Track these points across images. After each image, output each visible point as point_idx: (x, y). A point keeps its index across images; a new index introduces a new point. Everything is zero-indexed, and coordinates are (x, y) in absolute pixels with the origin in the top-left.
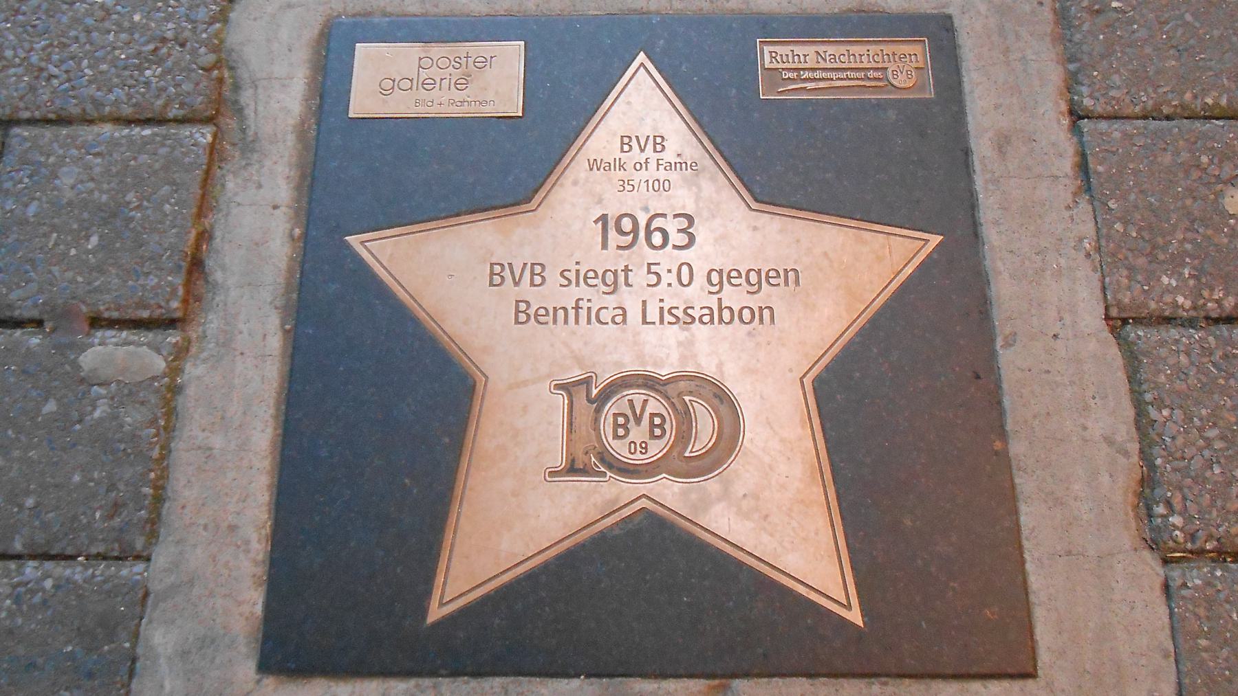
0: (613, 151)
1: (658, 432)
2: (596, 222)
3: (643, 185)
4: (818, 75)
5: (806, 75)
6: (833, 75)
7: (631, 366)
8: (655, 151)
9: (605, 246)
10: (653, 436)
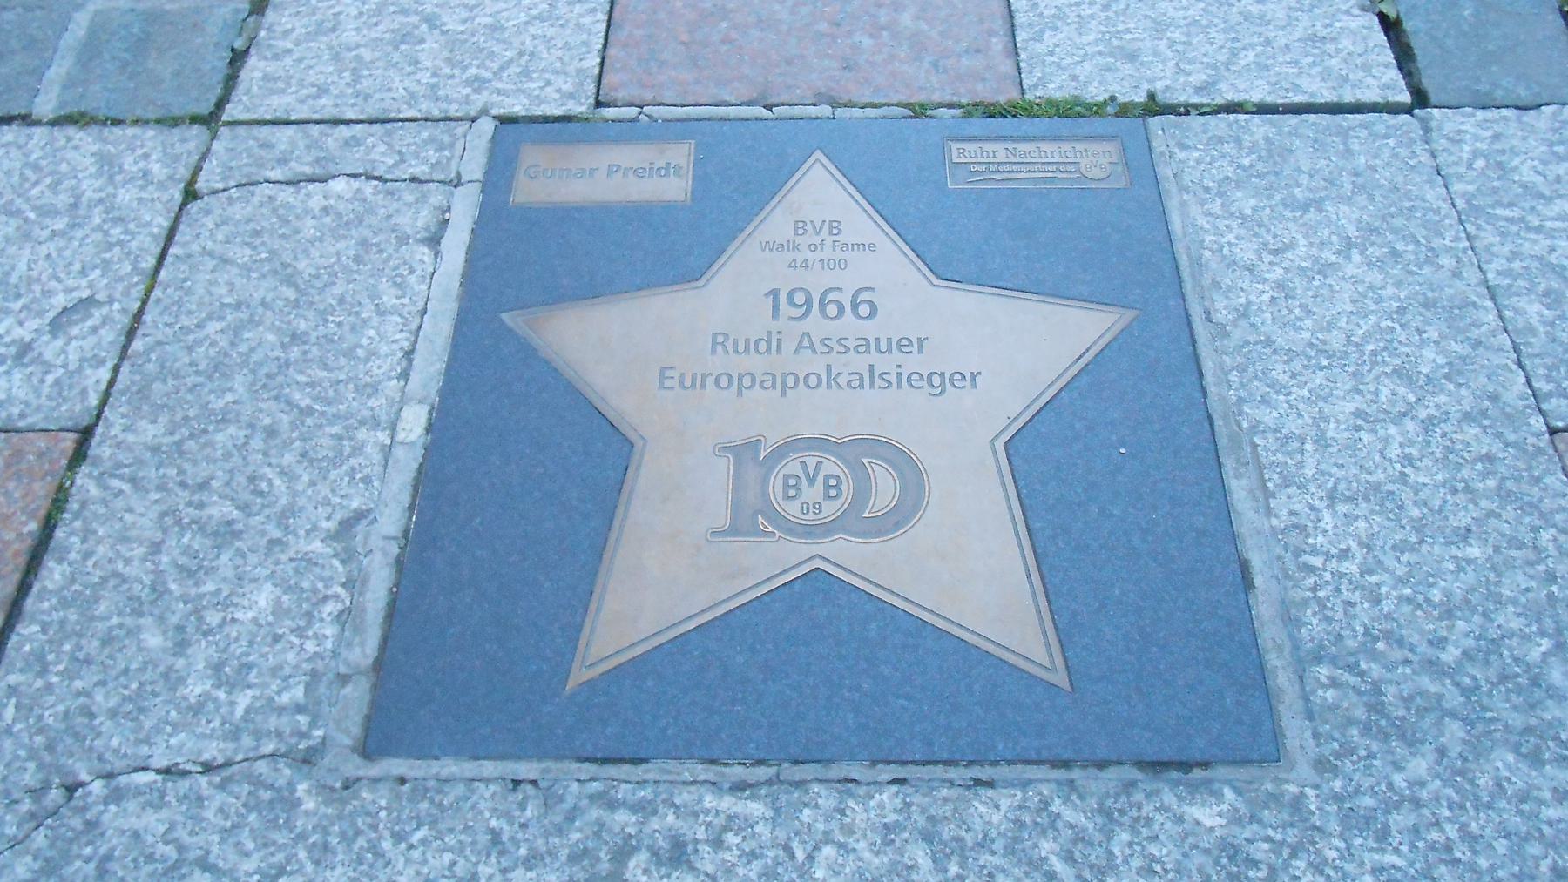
1: (833, 493)
2: (767, 295)
4: (1008, 168)
5: (995, 168)
6: (1022, 167)
7: (805, 430)
8: (831, 233)
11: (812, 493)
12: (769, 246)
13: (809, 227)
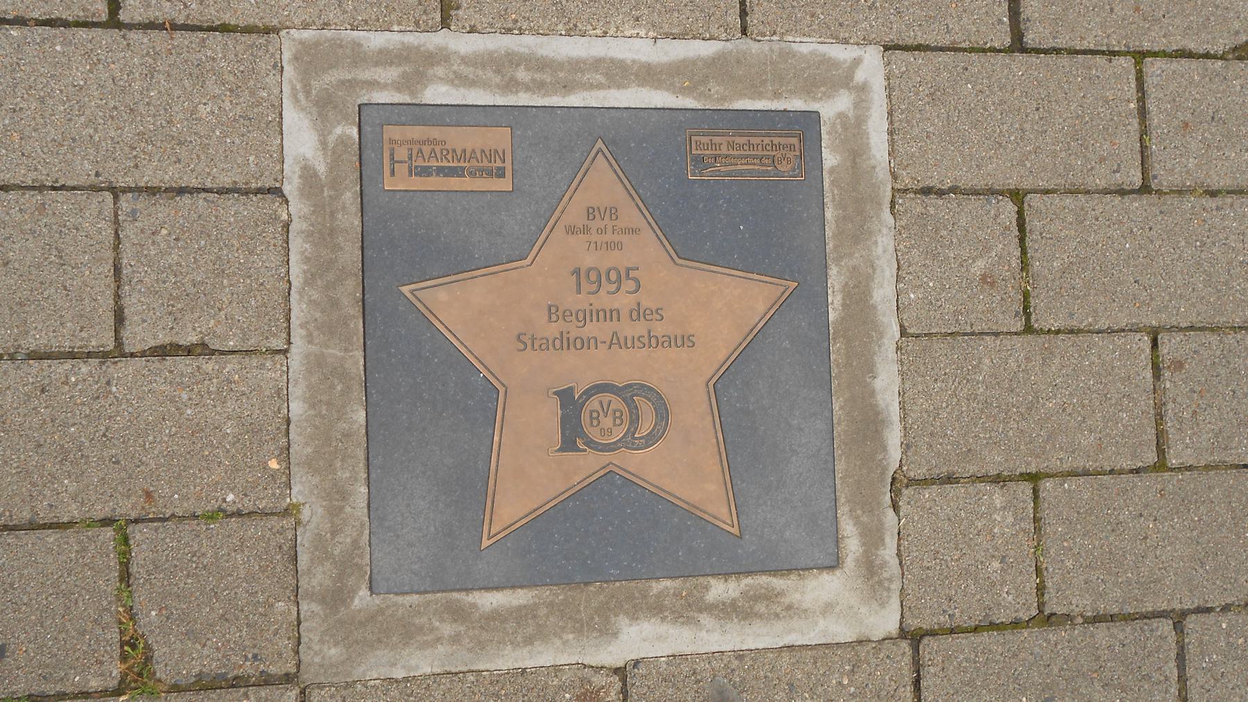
0: (581, 221)
1: (618, 421)
11: (607, 422)
12: (571, 230)
13: (596, 213)
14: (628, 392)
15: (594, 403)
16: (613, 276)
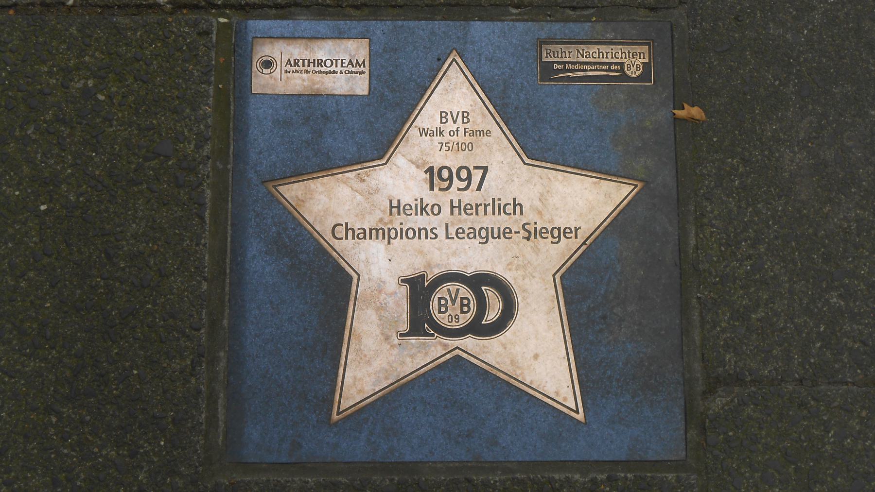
1: (465, 309)
2: (426, 172)
3: (455, 146)
4: (577, 67)
6: (588, 67)
8: (463, 122)
9: (432, 189)
10: (462, 312)
12: (424, 132)
13: (449, 116)
14: (478, 282)
15: (442, 291)
16: (464, 174)
